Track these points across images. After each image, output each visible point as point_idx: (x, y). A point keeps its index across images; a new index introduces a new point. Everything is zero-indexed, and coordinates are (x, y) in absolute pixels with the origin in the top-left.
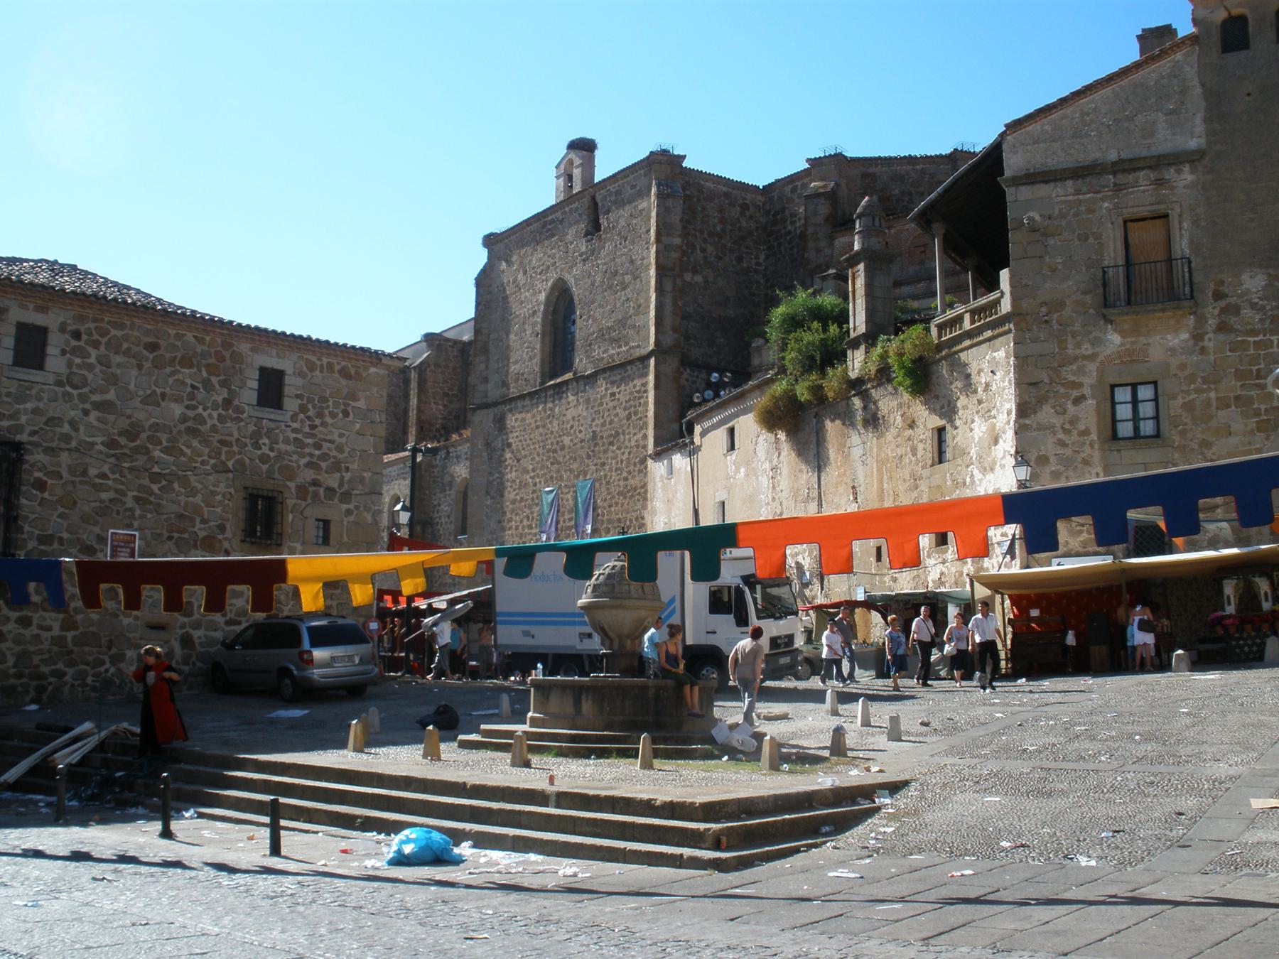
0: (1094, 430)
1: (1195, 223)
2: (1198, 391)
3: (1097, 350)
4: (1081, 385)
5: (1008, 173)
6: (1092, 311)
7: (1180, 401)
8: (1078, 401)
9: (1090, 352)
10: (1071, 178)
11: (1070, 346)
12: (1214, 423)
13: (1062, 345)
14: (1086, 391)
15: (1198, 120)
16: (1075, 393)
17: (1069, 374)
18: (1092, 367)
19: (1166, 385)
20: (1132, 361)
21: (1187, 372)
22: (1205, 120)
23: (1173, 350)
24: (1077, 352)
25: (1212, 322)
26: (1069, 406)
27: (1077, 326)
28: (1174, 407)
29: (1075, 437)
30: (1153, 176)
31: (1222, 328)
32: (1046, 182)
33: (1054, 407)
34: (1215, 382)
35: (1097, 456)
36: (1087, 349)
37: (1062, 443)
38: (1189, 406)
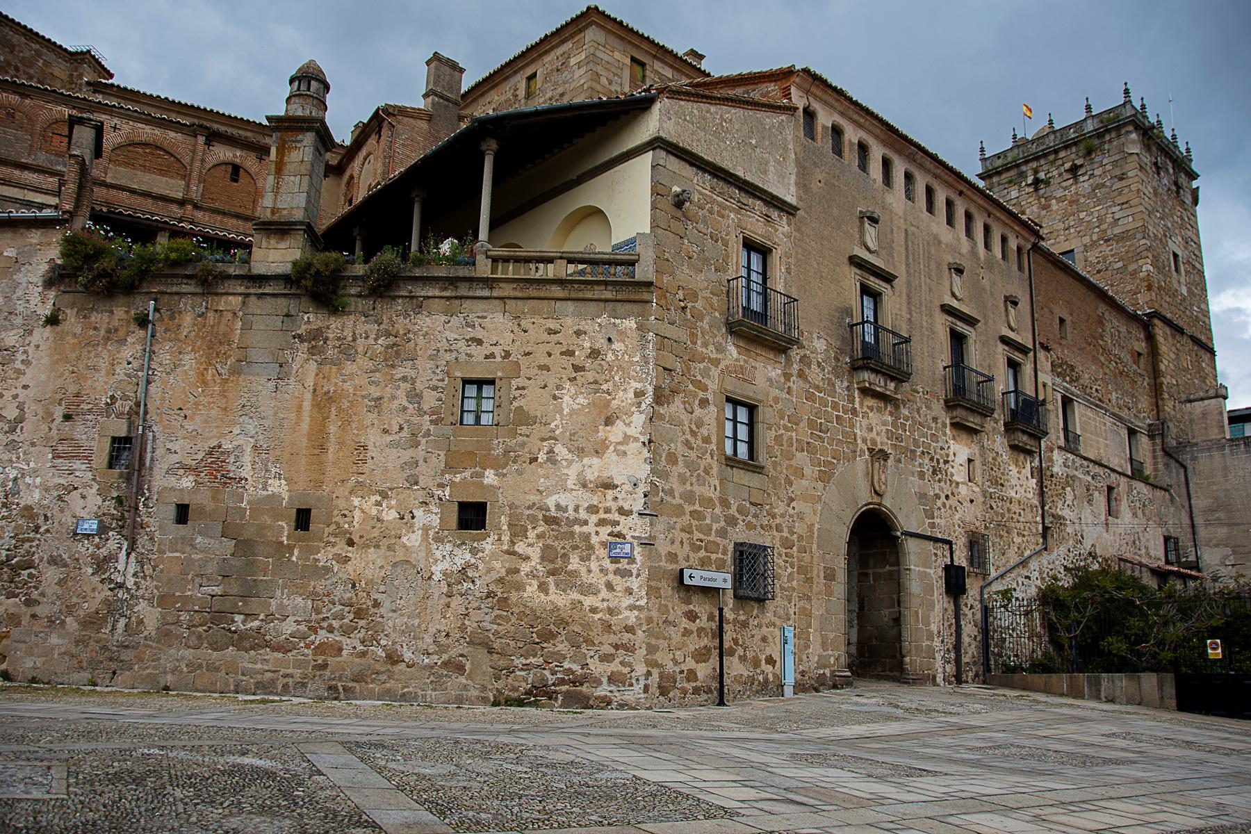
0: (714, 439)
1: (788, 271)
2: (786, 428)
3: (719, 356)
4: (705, 389)
6: (717, 314)
7: (772, 433)
8: (704, 403)
9: (714, 356)
10: (710, 173)
11: (699, 342)
12: (793, 462)
14: (711, 398)
15: (793, 177)
16: (701, 394)
18: (715, 372)
19: (764, 414)
20: (744, 380)
21: (779, 406)
22: (797, 184)
23: (770, 380)
24: (704, 350)
26: (696, 407)
27: (705, 324)
28: (766, 437)
29: (699, 442)
30: (765, 210)
31: (801, 375)
32: (691, 164)
33: (684, 403)
34: (797, 424)
36: (711, 352)
38: (778, 438)
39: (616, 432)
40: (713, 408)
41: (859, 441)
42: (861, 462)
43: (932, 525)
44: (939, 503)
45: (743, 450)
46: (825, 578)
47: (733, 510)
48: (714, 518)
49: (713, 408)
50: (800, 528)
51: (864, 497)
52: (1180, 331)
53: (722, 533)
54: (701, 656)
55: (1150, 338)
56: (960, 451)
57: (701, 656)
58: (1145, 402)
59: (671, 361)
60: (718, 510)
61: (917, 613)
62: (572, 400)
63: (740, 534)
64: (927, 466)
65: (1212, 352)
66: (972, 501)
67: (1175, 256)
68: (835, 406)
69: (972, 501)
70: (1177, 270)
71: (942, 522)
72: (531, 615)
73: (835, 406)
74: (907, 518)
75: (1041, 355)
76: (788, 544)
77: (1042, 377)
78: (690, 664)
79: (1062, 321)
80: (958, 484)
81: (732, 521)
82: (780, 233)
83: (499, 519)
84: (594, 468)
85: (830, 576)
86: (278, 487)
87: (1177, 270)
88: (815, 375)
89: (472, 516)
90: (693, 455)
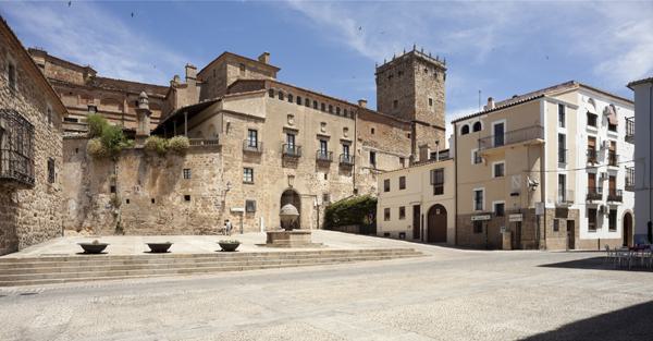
19: (255, 171)
22: (267, 111)
39: (214, 179)
42: (286, 178)
45: (250, 180)
48: (240, 196)
51: (286, 187)
52: (428, 125)
55: (414, 130)
56: (321, 175)
58: (410, 149)
62: (206, 172)
64: (309, 177)
65: (444, 130)
67: (430, 100)
70: (431, 104)
72: (200, 217)
74: (302, 191)
75: (358, 143)
77: (357, 148)
79: (373, 130)
82: (259, 126)
83: (192, 198)
84: (211, 187)
85: (275, 205)
86: (147, 194)
87: (431, 104)
88: (271, 160)
89: (187, 198)
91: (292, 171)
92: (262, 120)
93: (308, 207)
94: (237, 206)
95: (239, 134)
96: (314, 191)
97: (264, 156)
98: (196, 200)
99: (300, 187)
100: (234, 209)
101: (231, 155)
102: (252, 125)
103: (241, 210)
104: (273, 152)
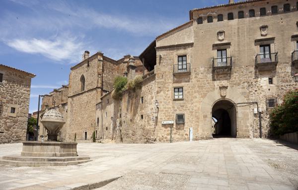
4: (168, 88)
5: (157, 46)
8: (168, 91)
12: (193, 96)
13: (165, 80)
17: (166, 85)
25: (194, 76)
27: (168, 76)
31: (196, 77)
35: (171, 102)
37: (164, 99)
38: (189, 92)
40: (170, 92)
41: (216, 86)
43: (249, 99)
44: (251, 93)
46: (204, 117)
47: (176, 108)
48: (171, 111)
49: (170, 92)
50: (195, 108)
51: (217, 98)
53: (173, 113)
54: (168, 135)
57: (168, 135)
59: (160, 86)
60: (172, 109)
61: (240, 122)
63: (178, 112)
66: (269, 89)
68: (207, 81)
69: (269, 89)
71: (253, 98)
73: (207, 81)
76: (192, 112)
78: (166, 136)
80: (262, 86)
81: (176, 110)
82: (189, 51)
85: (205, 117)
88: (200, 76)
90: (165, 101)
91: (224, 83)
92: (191, 45)
93: (246, 115)
94: (169, 119)
95: (169, 62)
96: (253, 98)
97: (193, 75)
98: (145, 118)
99: (234, 95)
100: (165, 123)
101: (163, 80)
102: (181, 52)
103: (170, 122)
104: (202, 69)
